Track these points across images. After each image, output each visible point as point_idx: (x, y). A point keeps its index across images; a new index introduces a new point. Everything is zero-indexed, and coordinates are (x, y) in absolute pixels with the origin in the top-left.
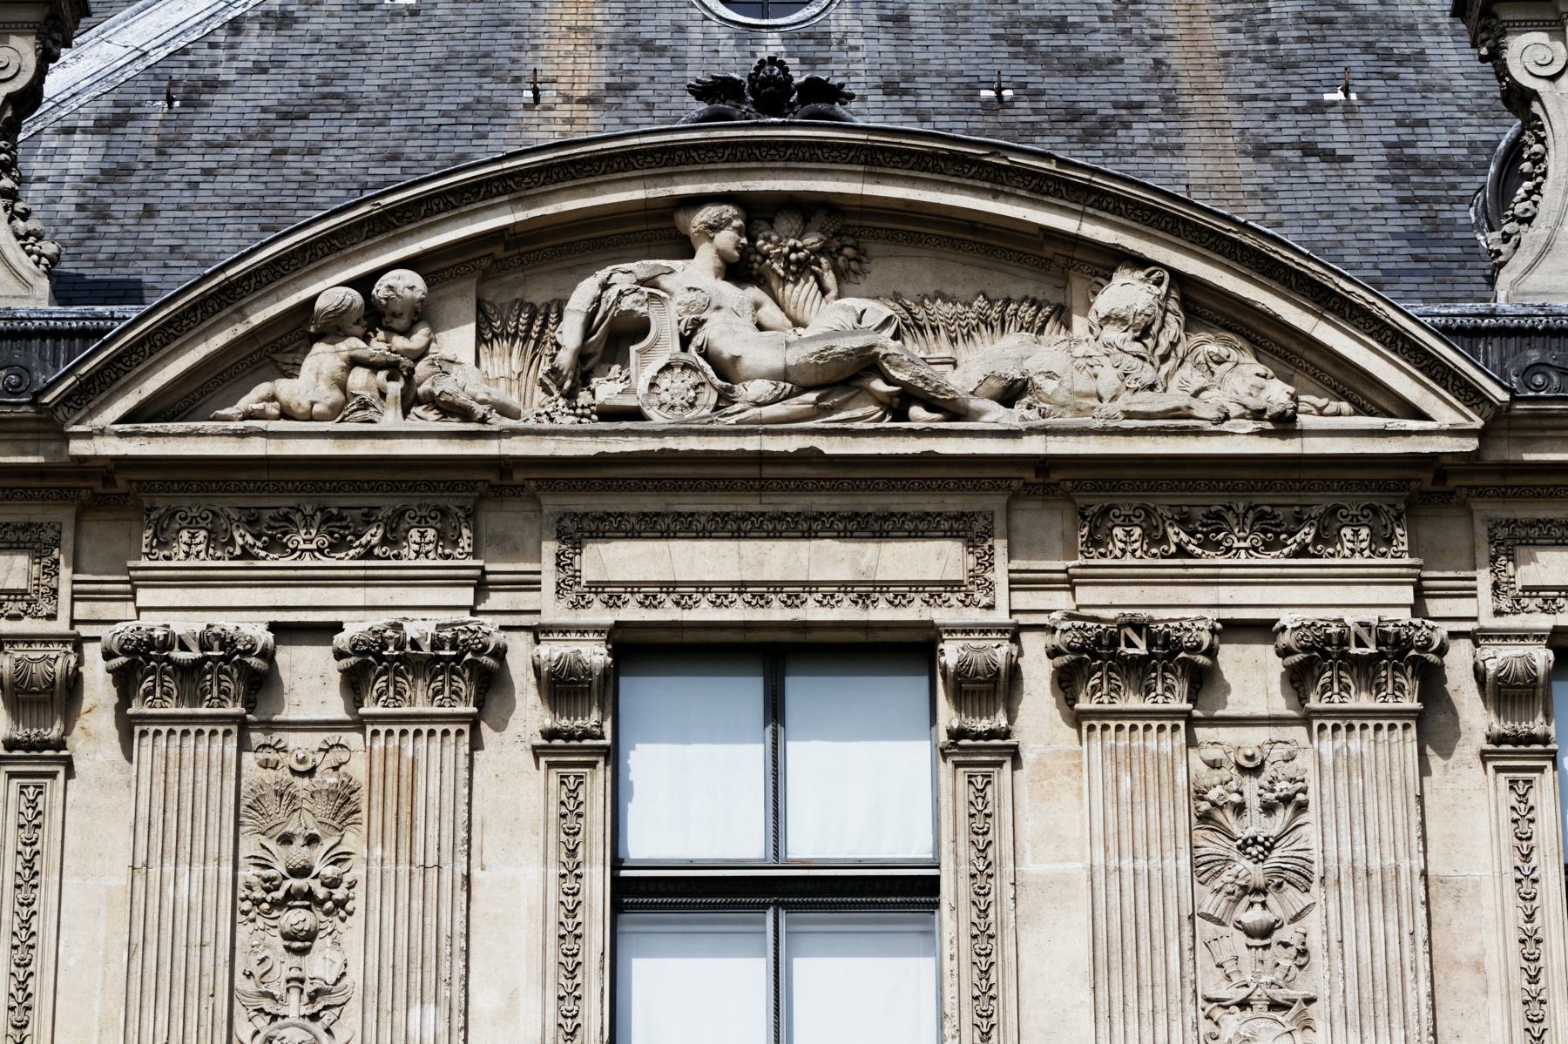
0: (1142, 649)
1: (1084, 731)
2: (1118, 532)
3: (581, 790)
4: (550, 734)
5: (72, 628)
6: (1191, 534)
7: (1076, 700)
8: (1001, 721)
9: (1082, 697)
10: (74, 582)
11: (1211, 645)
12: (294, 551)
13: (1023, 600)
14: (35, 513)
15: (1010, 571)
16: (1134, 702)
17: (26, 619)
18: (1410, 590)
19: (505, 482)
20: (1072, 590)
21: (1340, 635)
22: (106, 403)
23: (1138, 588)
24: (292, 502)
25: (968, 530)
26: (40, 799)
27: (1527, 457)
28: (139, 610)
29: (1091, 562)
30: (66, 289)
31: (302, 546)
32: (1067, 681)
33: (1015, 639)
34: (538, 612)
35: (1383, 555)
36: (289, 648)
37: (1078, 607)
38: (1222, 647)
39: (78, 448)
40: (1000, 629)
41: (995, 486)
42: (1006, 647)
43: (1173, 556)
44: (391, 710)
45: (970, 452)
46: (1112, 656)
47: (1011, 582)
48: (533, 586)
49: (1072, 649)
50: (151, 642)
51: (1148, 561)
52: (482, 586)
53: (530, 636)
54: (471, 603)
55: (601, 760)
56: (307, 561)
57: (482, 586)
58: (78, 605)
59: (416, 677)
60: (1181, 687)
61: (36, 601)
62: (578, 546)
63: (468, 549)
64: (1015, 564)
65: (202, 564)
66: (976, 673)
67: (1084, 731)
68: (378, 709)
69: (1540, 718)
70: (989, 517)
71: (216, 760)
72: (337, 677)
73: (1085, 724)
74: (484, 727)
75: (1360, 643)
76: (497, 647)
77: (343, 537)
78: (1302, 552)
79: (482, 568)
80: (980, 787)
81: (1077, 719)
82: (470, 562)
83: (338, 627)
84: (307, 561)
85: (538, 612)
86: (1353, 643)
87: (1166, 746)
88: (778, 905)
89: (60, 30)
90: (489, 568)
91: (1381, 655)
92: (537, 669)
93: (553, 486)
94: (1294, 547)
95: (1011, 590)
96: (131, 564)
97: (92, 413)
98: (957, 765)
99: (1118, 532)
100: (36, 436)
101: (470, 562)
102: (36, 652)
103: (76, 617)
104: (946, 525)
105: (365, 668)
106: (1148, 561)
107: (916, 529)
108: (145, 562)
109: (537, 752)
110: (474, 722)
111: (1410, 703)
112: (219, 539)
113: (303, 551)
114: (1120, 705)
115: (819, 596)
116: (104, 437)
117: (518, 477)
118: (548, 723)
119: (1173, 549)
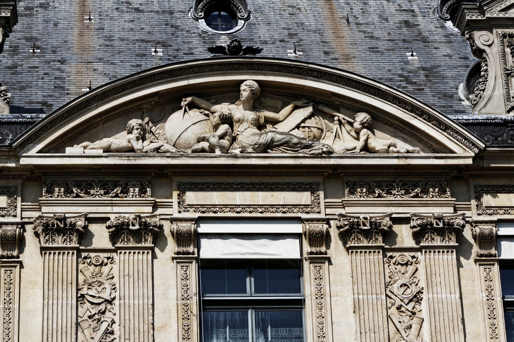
0: (441, 225)
1: (350, 253)
2: (359, 190)
3: (321, 271)
4: (178, 253)
5: (21, 219)
6: (383, 191)
7: (347, 244)
8: (323, 249)
9: (349, 243)
10: (22, 205)
11: (390, 225)
12: (93, 195)
13: (329, 211)
14: (12, 183)
15: (325, 202)
16: (365, 244)
17: (6, 217)
18: (452, 208)
19: (161, 173)
20: (344, 208)
21: (358, 222)
22: (33, 147)
23: (367, 209)
24: (92, 179)
25: (313, 189)
26: (11, 275)
27: (492, 165)
28: (42, 213)
29: (369, 199)
30: (13, 109)
31: (396, 193)
32: (344, 236)
33: (328, 223)
34: (172, 215)
35: (69, 197)
36: (396, 226)
37: (346, 213)
38: (90, 225)
39: (23, 161)
40: (323, 220)
41: (320, 174)
42: (326, 226)
43: (377, 197)
44: (126, 245)
45: (94, 163)
46: (431, 229)
47: (325, 206)
48: (171, 206)
49: (115, 226)
50: (123, 223)
51: (140, 199)
52: (155, 206)
53: (169, 221)
54: (151, 211)
55: (194, 262)
56: (97, 198)
57: (155, 206)
58: (23, 212)
59: (59, 235)
60: (380, 239)
61: (9, 211)
62: (184, 193)
63: (150, 195)
64: (327, 200)
65: (365, 199)
66: (184, 234)
67: (350, 253)
68: (122, 245)
69: (493, 249)
70: (318, 184)
71: (136, 261)
72: (107, 235)
73: (350, 251)
74: (157, 250)
75: (133, 225)
76: (160, 225)
77: (108, 190)
78: (417, 196)
79: (155, 200)
80: (185, 270)
81: (348, 249)
82: (150, 199)
83: (108, 219)
84: (97, 198)
85: (172, 215)
86: (362, 225)
87: (450, 257)
88: (253, 308)
89: (9, 27)
90: (157, 200)
91: (140, 229)
92: (172, 233)
93: (175, 174)
94: (414, 194)
95: (325, 208)
96: (41, 199)
97: (28, 150)
98: (310, 263)
99: (431, 190)
100: (6, 157)
101: (150, 199)
102: (9, 228)
103: (23, 216)
104: (200, 187)
105: (118, 232)
106: (140, 199)
107: (225, 188)
108: (44, 198)
109: (173, 259)
110: (152, 249)
111: (453, 243)
112: (68, 192)
113: (96, 195)
114: (435, 244)
115: (194, 209)
116: (33, 157)
117: (166, 171)
118: (177, 249)
119: (75, 195)
